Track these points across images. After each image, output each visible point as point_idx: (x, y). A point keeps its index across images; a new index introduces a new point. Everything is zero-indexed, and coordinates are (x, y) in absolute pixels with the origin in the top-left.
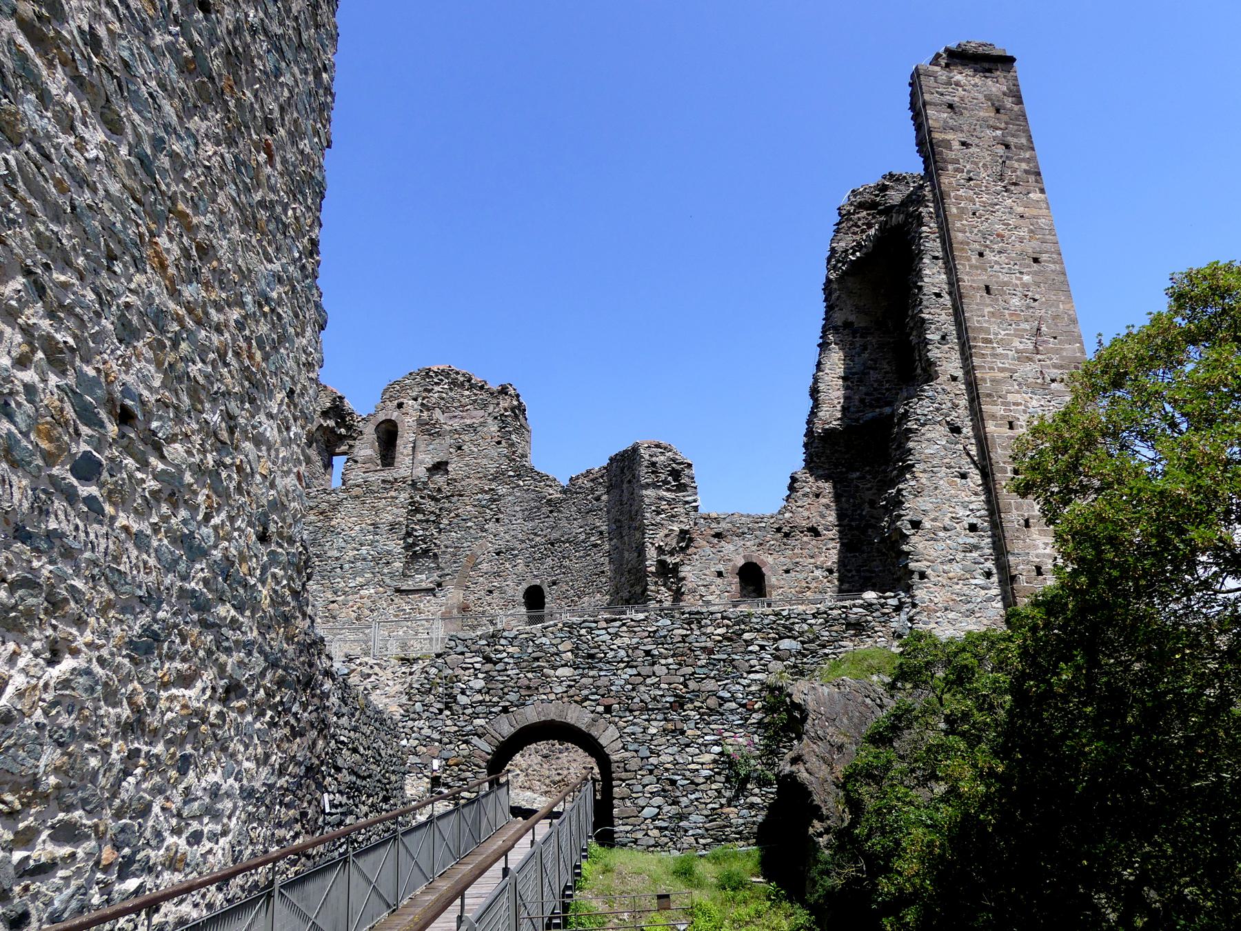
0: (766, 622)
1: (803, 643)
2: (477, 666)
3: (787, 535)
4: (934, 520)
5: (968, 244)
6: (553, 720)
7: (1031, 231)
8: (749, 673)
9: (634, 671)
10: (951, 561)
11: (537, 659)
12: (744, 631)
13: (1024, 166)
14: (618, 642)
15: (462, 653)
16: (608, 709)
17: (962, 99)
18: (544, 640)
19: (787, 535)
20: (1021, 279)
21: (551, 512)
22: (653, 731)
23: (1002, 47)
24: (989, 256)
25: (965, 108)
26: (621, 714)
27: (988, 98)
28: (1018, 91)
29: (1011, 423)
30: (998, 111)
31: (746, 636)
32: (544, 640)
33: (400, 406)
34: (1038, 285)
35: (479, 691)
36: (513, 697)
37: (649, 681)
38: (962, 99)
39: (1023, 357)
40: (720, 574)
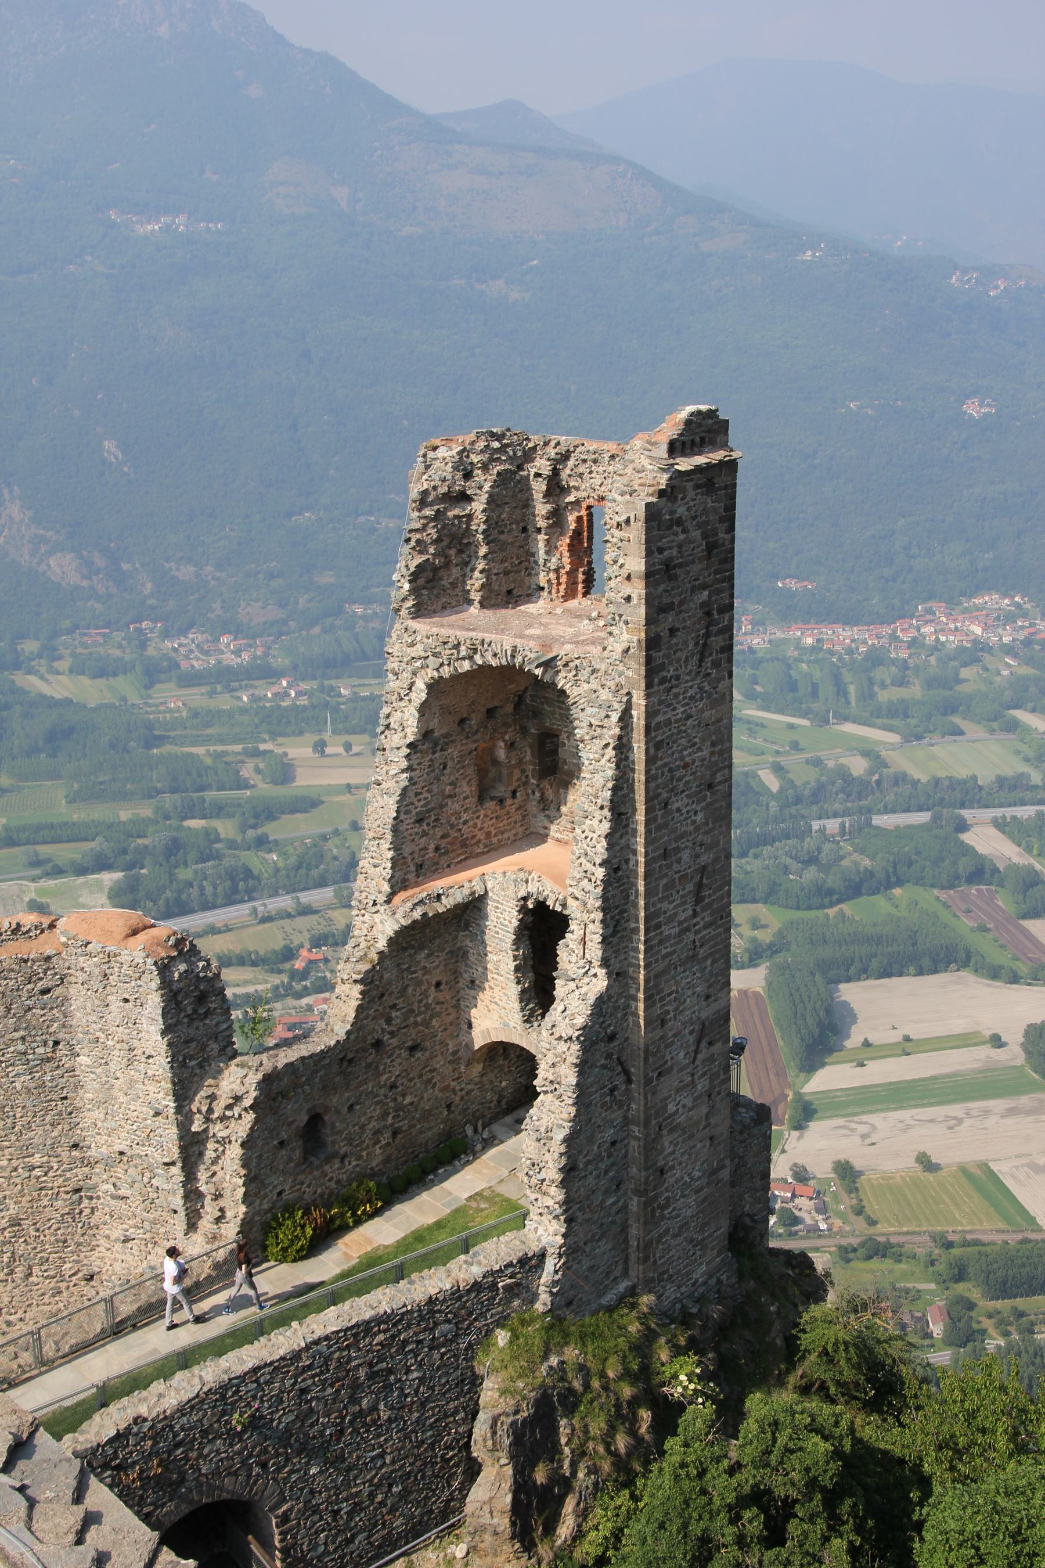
3: (351, 1061)
7: (713, 745)
17: (680, 546)
25: (680, 565)
30: (709, 556)
38: (680, 546)
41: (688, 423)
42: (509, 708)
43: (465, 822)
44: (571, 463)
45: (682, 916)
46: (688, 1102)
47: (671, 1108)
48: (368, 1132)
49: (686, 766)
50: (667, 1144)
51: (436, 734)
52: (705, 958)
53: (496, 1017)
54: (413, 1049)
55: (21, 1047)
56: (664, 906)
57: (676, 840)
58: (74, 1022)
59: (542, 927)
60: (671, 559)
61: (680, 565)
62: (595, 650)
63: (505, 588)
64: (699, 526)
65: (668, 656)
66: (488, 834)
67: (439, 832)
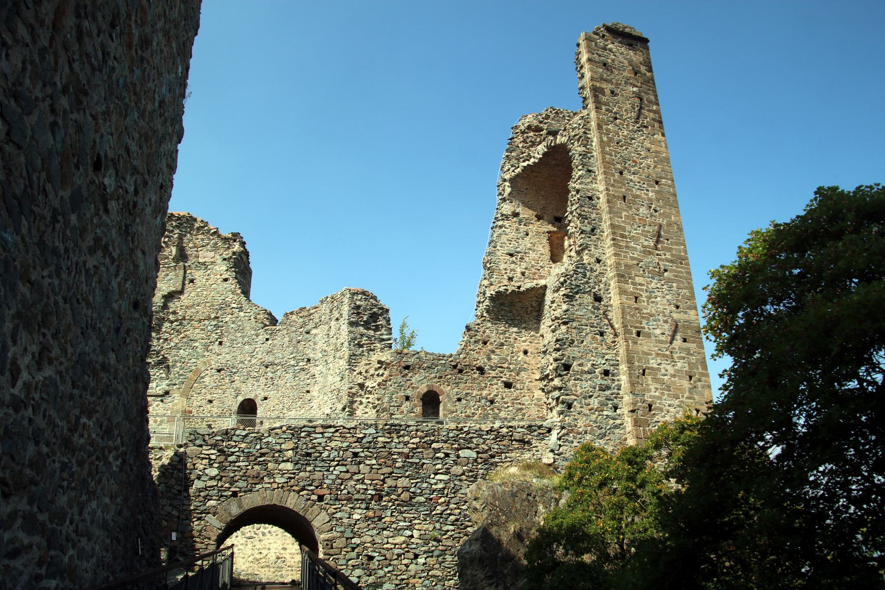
0: (451, 435)
1: (478, 453)
2: (213, 457)
4: (581, 365)
5: (614, 164)
6: (275, 505)
7: (655, 162)
8: (436, 474)
9: (344, 469)
10: (590, 397)
11: (263, 455)
12: (433, 441)
13: (651, 114)
14: (333, 444)
15: (201, 446)
16: (321, 498)
17: (613, 60)
18: (270, 439)
19: (461, 371)
20: (647, 195)
21: (267, 340)
22: (356, 517)
23: (640, 30)
26: (331, 502)
27: (631, 63)
28: (650, 63)
29: (636, 298)
30: (636, 74)
31: (434, 445)
32: (270, 439)
34: (658, 200)
35: (212, 478)
36: (242, 484)
37: (356, 477)
38: (613, 60)
39: (647, 252)
40: (407, 398)
43: (542, 267)
46: (671, 370)
50: (652, 387)
52: (672, 281)
55: (293, 362)
56: (628, 228)
67: (524, 265)
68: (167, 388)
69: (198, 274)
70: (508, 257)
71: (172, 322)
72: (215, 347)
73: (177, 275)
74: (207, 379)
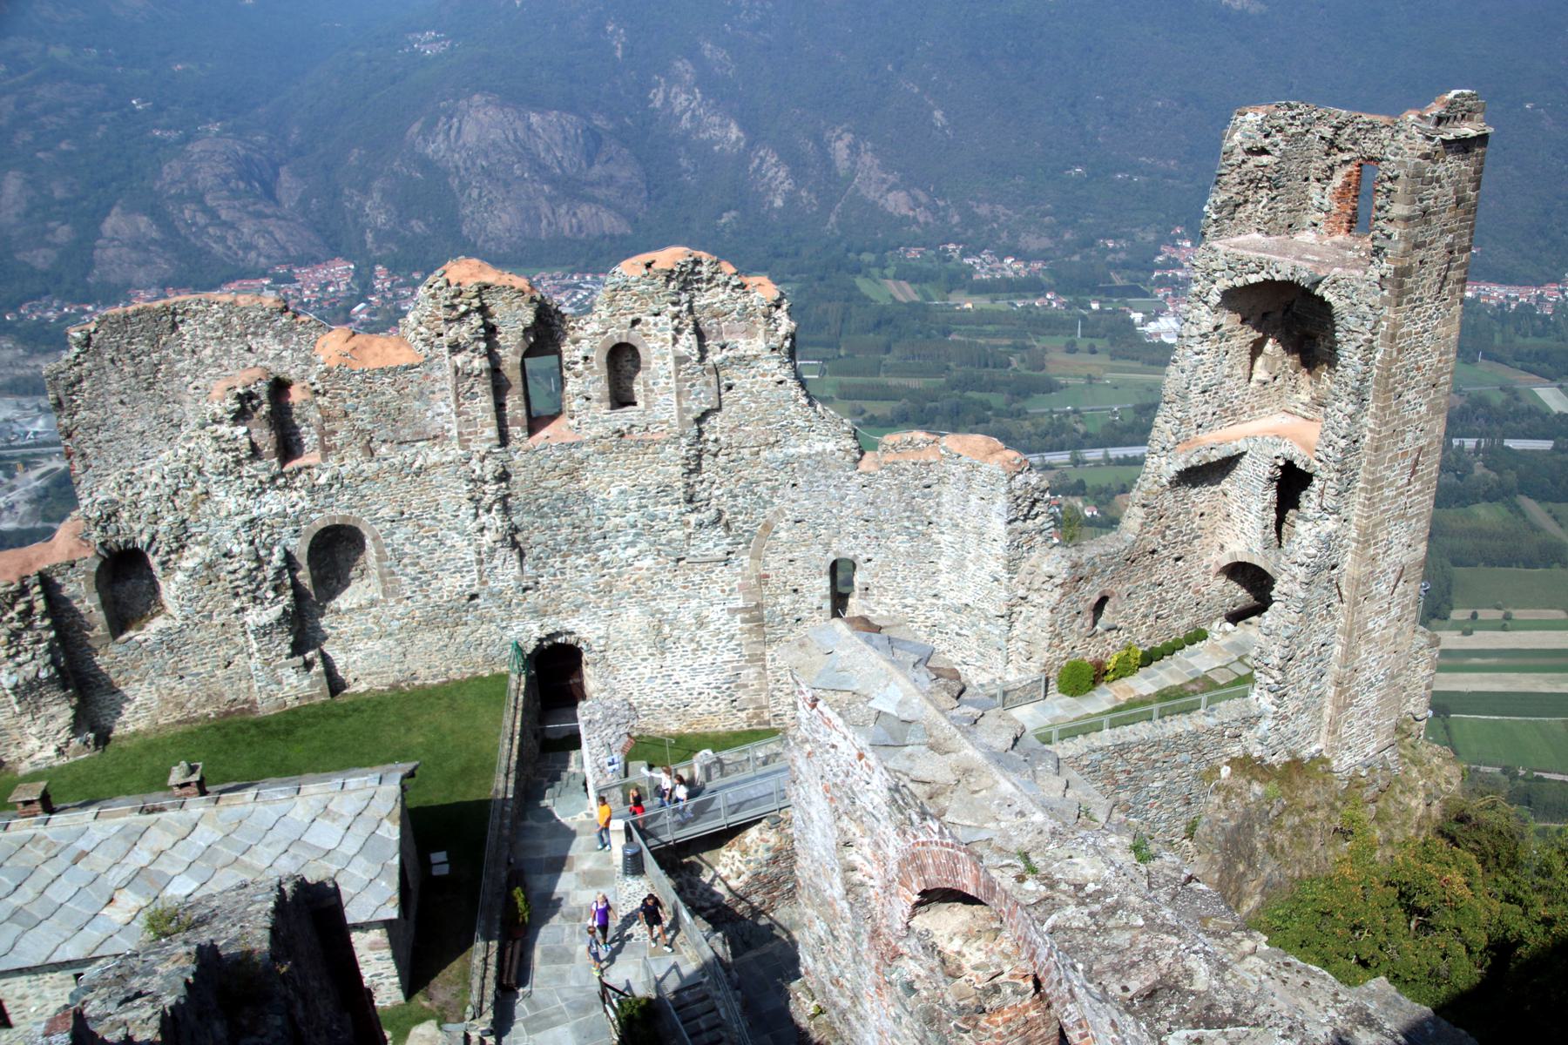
7: (1441, 354)
24: (1409, 395)
25: (1434, 213)
33: (635, 322)
41: (1452, 103)
42: (1279, 315)
44: (1349, 130)
45: (1400, 483)
47: (1370, 626)
48: (1139, 615)
49: (1418, 369)
51: (1223, 329)
53: (1243, 543)
54: (1177, 559)
55: (907, 524)
56: (1387, 473)
57: (1404, 424)
58: (943, 510)
59: (1291, 483)
60: (1428, 207)
61: (1434, 213)
62: (1358, 273)
63: (1287, 223)
64: (1453, 184)
65: (1415, 282)
66: (1252, 408)
68: (730, 549)
69: (737, 376)
70: (1201, 398)
71: (715, 455)
72: (790, 493)
73: (707, 384)
74: (783, 534)
